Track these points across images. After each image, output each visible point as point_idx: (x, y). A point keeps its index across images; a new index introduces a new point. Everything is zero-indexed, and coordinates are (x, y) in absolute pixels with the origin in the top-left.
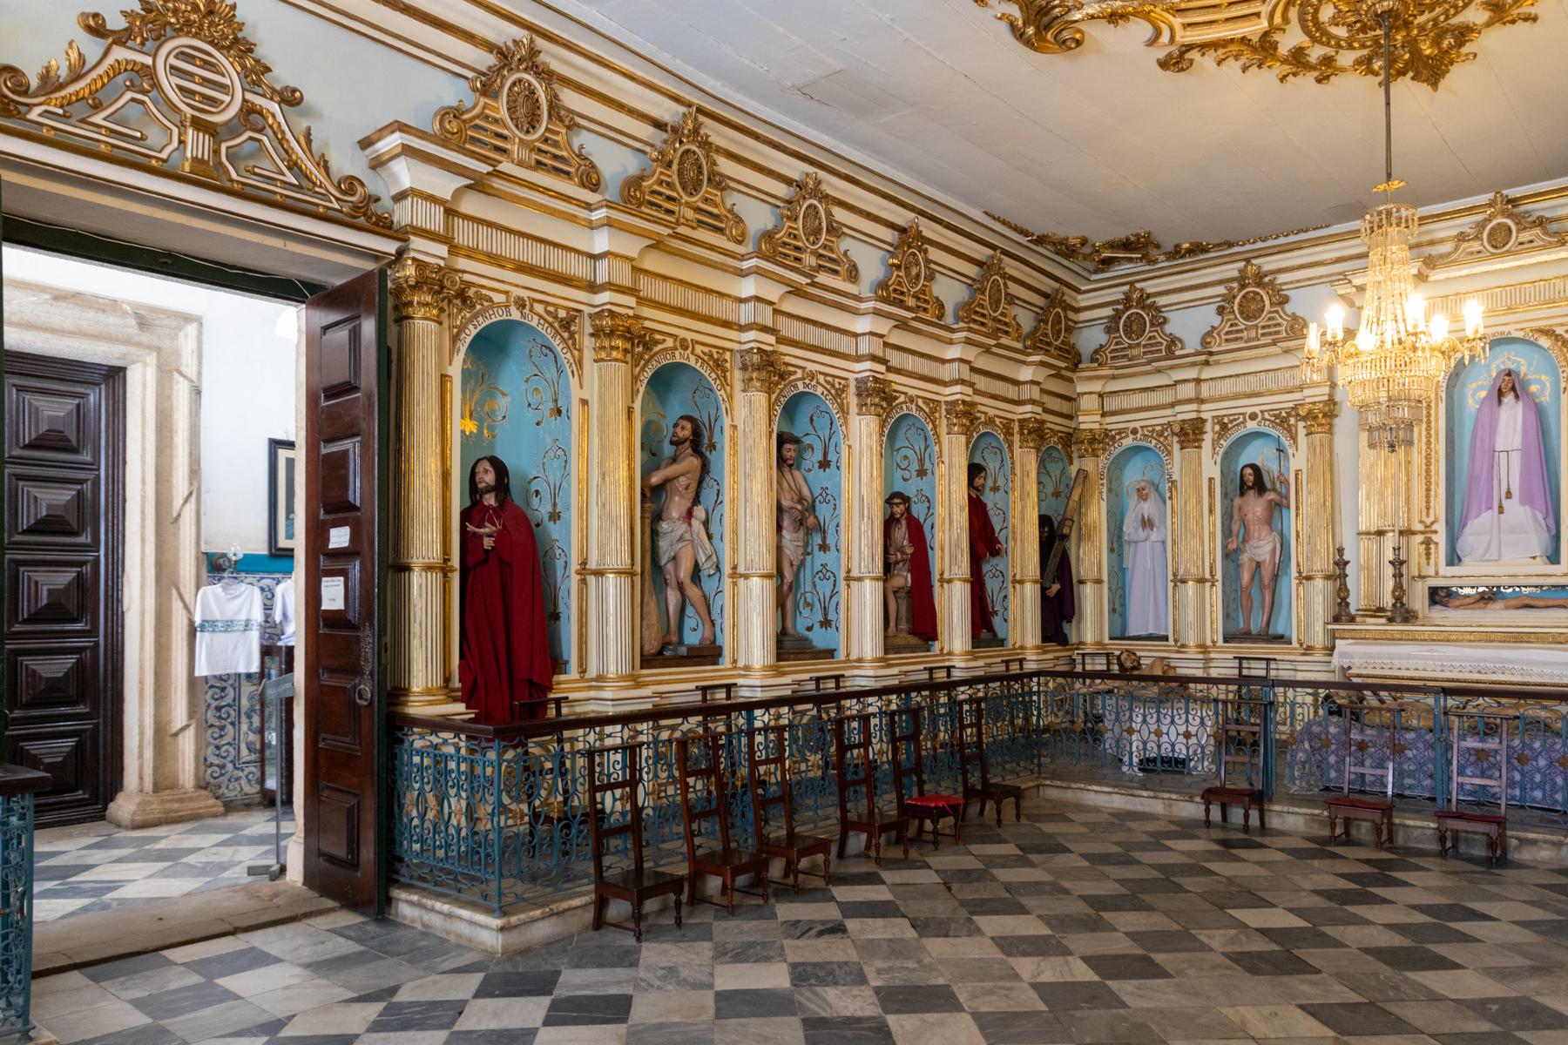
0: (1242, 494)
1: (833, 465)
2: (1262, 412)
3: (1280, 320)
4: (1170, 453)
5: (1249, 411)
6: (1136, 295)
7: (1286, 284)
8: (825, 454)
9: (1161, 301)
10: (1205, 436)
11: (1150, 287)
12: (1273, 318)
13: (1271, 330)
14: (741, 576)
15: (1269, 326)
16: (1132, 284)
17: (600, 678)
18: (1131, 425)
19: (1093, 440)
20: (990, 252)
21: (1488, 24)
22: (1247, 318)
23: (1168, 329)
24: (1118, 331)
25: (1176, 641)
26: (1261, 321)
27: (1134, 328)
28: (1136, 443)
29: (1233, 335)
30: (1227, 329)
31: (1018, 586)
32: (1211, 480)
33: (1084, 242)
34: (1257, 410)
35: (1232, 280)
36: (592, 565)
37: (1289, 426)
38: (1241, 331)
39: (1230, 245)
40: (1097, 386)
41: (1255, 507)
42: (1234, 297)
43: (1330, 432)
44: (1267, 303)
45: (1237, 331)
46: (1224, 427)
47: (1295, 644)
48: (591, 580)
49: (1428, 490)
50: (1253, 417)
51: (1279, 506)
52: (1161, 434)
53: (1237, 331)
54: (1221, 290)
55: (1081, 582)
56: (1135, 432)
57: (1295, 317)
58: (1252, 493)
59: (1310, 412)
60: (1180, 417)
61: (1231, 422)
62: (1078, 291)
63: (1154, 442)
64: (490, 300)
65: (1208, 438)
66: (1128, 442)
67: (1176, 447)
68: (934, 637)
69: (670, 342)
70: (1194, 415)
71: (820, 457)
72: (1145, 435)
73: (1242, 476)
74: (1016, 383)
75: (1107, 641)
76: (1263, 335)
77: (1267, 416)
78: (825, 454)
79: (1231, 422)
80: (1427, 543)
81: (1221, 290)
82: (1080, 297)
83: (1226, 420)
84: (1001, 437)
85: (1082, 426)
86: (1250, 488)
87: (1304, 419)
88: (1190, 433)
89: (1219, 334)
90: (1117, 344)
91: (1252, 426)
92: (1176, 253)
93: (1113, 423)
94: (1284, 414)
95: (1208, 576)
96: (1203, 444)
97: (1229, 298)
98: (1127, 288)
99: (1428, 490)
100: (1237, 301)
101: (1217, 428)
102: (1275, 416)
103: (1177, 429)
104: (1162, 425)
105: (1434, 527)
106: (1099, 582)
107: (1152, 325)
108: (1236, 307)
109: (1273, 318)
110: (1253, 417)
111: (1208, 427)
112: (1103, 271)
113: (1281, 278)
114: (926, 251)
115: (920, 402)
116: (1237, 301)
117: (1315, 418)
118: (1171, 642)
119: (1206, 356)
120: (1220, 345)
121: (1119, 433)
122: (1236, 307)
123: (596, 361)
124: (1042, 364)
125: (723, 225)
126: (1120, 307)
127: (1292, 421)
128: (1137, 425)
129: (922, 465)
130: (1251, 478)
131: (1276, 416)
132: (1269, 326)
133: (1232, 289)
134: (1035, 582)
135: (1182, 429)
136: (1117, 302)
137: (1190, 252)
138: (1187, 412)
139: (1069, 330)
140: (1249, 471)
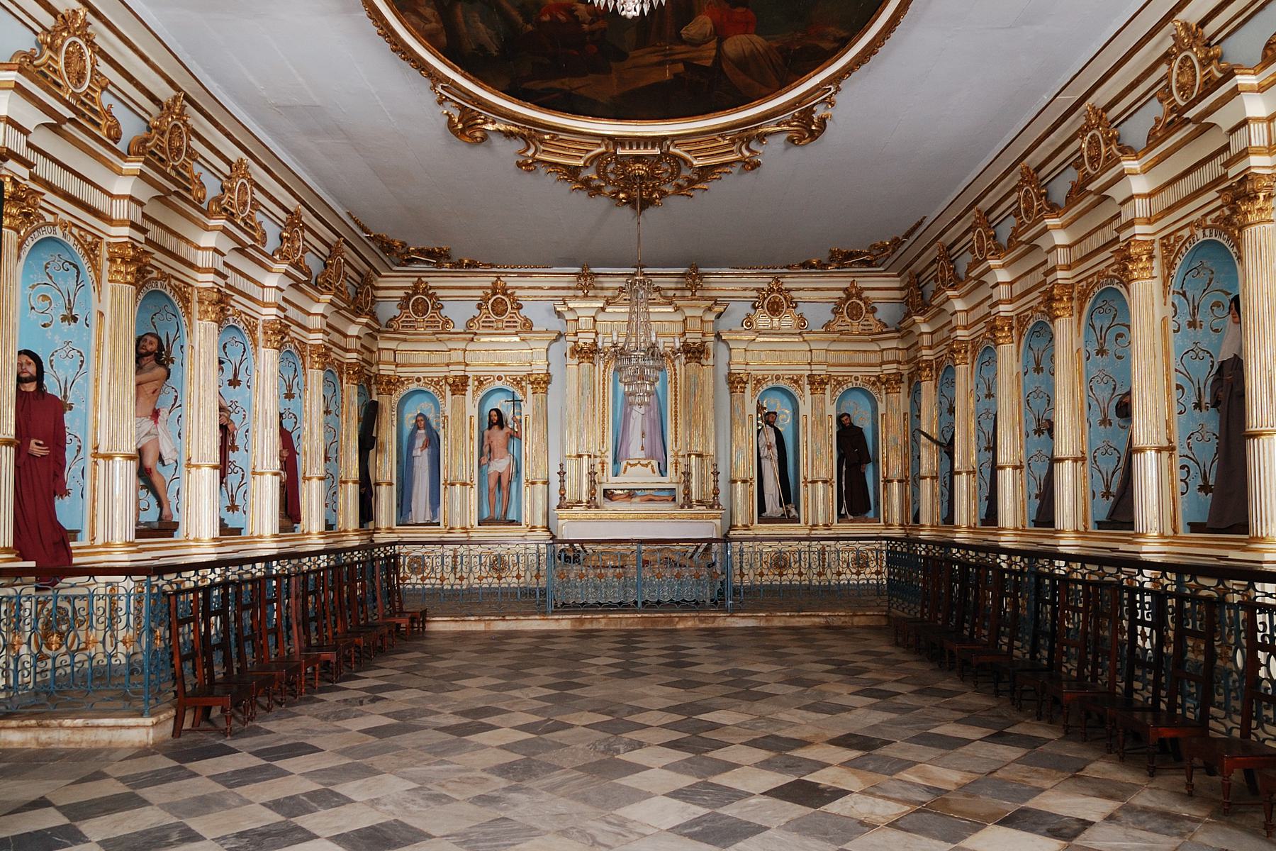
0: (490, 428)
1: (243, 384)
2: (506, 376)
3: (517, 319)
4: (444, 397)
5: (497, 374)
6: (423, 285)
7: (521, 297)
8: (235, 375)
9: (439, 293)
10: (468, 388)
11: (433, 282)
12: (513, 317)
13: (511, 324)
14: (194, 466)
15: (510, 322)
16: (419, 277)
17: (107, 545)
18: (417, 375)
19: (389, 382)
20: (336, 238)
21: (673, 193)
22: (497, 315)
23: (443, 312)
24: (408, 308)
25: (446, 526)
26: (505, 318)
27: (421, 309)
28: (419, 388)
29: (488, 324)
30: (483, 319)
31: (343, 485)
32: (471, 417)
33: (404, 245)
34: (502, 374)
35: (488, 288)
36: (102, 450)
37: (522, 387)
38: (493, 322)
39: (492, 266)
40: (393, 345)
41: (498, 436)
42: (489, 299)
43: (546, 393)
44: (509, 306)
45: (490, 322)
46: (481, 383)
47: (524, 525)
48: (101, 462)
49: (603, 432)
50: (500, 378)
51: (514, 436)
52: (437, 383)
53: (490, 322)
54: (480, 293)
55: (377, 484)
56: (418, 380)
57: (526, 319)
58: (496, 427)
59: (536, 379)
60: (453, 374)
61: (485, 380)
62: (380, 275)
63: (432, 388)
64: (43, 218)
65: (470, 389)
66: (413, 386)
67: (448, 393)
68: (299, 521)
69: (155, 274)
70: (462, 373)
71: (231, 377)
72: (426, 383)
73: (490, 416)
74: (346, 336)
75: (395, 527)
76: (507, 327)
77: (508, 379)
78: (235, 375)
79: (485, 380)
80: (603, 463)
81: (480, 293)
82: (380, 279)
83: (482, 379)
84: (337, 374)
85: (382, 372)
86: (495, 424)
87: (532, 383)
88: (459, 386)
89: (478, 321)
90: (407, 317)
91: (498, 384)
92: (459, 264)
93: (403, 372)
94: (518, 379)
95: (468, 482)
96: (467, 393)
97: (485, 299)
98: (416, 279)
99: (603, 432)
100: (491, 302)
101: (476, 383)
102: (513, 379)
103: (450, 381)
104: (438, 377)
105: (606, 454)
106: (391, 484)
107: (433, 308)
108: (489, 306)
109: (513, 317)
110: (500, 378)
111: (470, 382)
112: (404, 266)
113: (518, 293)
114: (304, 232)
115: (296, 342)
116: (491, 302)
117: (539, 383)
118: (442, 526)
119: (470, 334)
120: (478, 329)
121: (407, 380)
122: (489, 306)
123: (110, 281)
124: (367, 325)
125: (191, 187)
126: (410, 292)
127: (524, 383)
128: (421, 375)
129: (290, 390)
130: (496, 418)
131: (514, 380)
132: (510, 322)
133: (487, 294)
134: (355, 482)
135: (454, 381)
136: (408, 288)
137: (468, 265)
138: (457, 371)
139: (373, 302)
140: (494, 413)
